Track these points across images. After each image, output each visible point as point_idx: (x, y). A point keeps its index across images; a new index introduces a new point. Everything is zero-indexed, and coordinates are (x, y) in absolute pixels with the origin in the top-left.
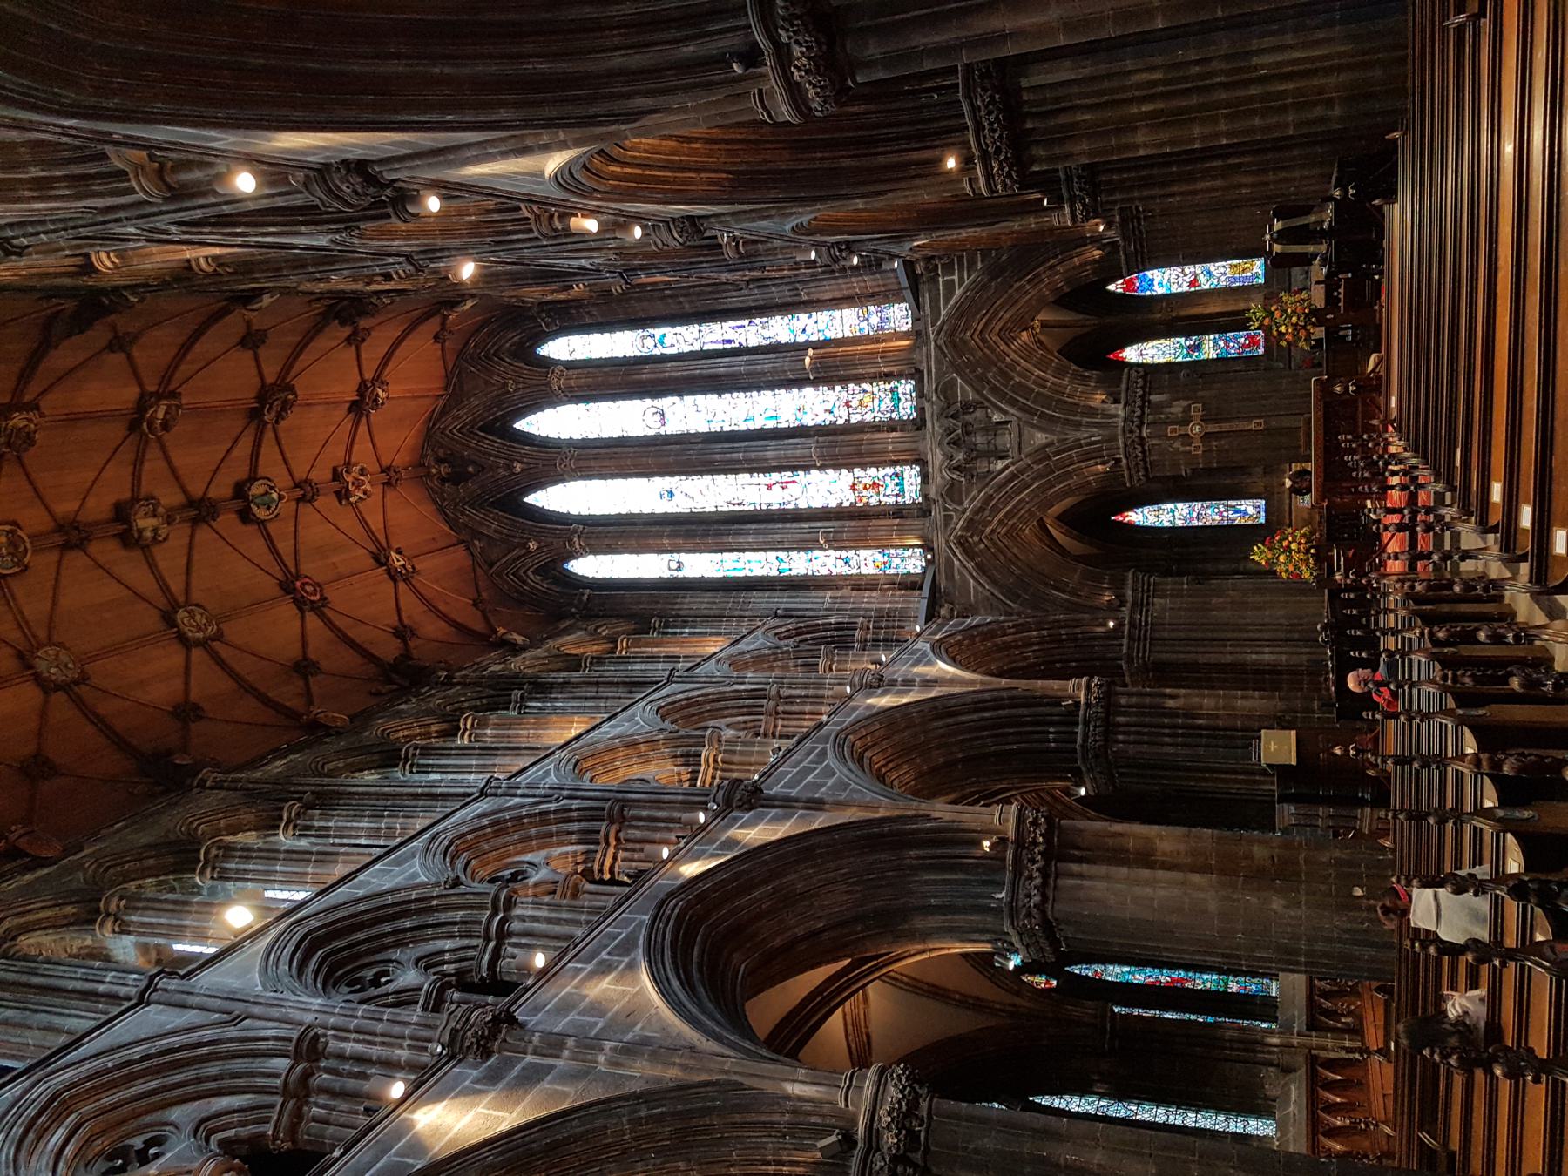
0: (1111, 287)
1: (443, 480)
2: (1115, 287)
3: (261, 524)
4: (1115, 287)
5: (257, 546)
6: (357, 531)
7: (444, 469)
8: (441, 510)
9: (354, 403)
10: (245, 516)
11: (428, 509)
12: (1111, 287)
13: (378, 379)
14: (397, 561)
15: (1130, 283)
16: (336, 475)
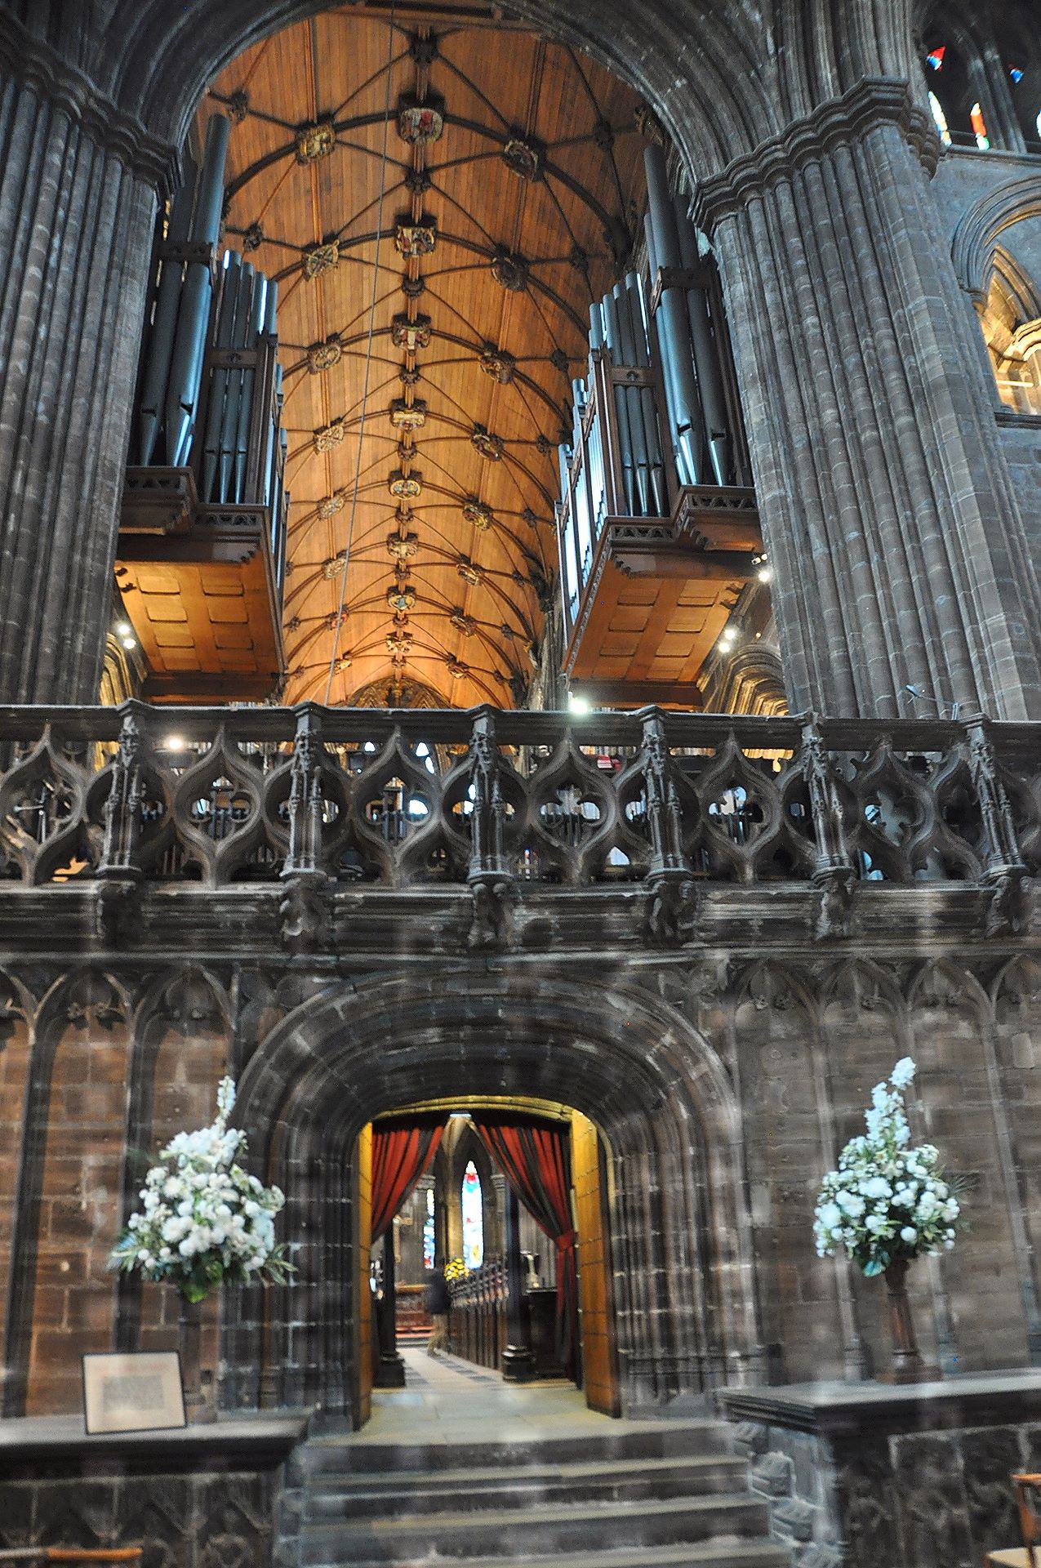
0: (471, 1165)
1: (390, 690)
2: (471, 1168)
3: (388, 596)
4: (471, 1168)
5: (373, 593)
6: (367, 642)
7: (397, 693)
8: (367, 687)
9: (455, 658)
10: (394, 590)
11: (373, 678)
12: (471, 1165)
13: (469, 675)
14: (344, 665)
15: (472, 1178)
16: (407, 636)
